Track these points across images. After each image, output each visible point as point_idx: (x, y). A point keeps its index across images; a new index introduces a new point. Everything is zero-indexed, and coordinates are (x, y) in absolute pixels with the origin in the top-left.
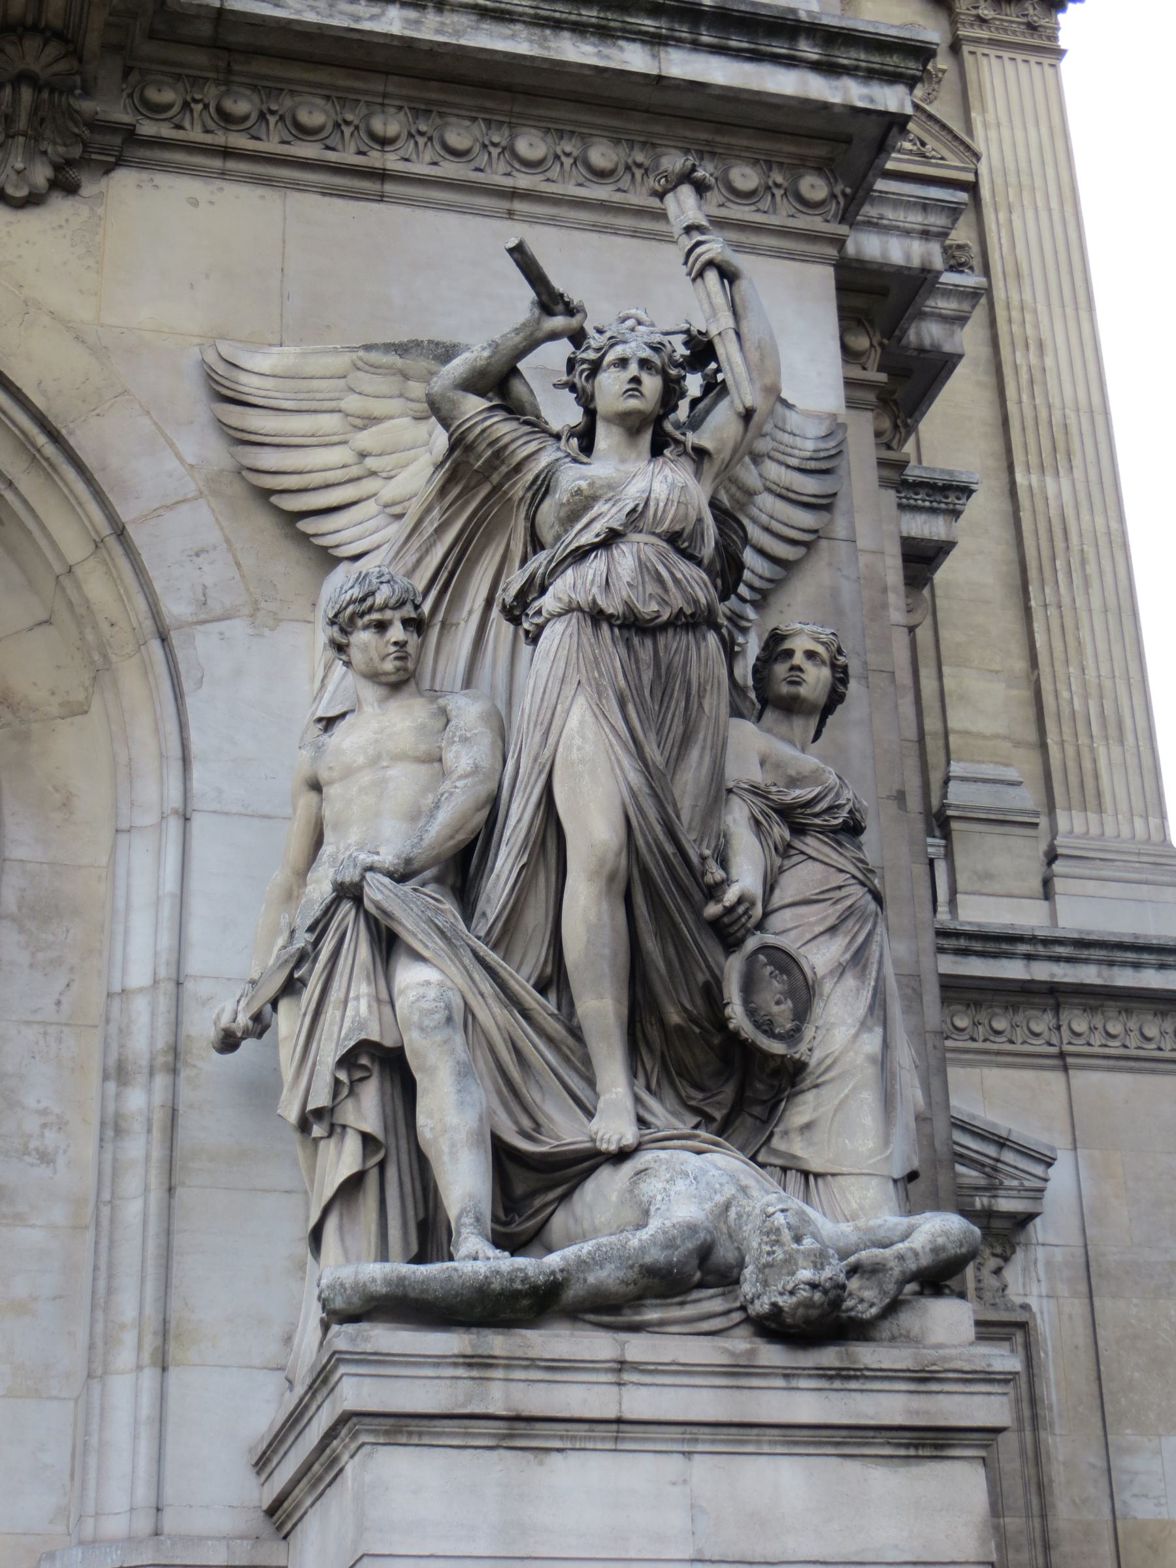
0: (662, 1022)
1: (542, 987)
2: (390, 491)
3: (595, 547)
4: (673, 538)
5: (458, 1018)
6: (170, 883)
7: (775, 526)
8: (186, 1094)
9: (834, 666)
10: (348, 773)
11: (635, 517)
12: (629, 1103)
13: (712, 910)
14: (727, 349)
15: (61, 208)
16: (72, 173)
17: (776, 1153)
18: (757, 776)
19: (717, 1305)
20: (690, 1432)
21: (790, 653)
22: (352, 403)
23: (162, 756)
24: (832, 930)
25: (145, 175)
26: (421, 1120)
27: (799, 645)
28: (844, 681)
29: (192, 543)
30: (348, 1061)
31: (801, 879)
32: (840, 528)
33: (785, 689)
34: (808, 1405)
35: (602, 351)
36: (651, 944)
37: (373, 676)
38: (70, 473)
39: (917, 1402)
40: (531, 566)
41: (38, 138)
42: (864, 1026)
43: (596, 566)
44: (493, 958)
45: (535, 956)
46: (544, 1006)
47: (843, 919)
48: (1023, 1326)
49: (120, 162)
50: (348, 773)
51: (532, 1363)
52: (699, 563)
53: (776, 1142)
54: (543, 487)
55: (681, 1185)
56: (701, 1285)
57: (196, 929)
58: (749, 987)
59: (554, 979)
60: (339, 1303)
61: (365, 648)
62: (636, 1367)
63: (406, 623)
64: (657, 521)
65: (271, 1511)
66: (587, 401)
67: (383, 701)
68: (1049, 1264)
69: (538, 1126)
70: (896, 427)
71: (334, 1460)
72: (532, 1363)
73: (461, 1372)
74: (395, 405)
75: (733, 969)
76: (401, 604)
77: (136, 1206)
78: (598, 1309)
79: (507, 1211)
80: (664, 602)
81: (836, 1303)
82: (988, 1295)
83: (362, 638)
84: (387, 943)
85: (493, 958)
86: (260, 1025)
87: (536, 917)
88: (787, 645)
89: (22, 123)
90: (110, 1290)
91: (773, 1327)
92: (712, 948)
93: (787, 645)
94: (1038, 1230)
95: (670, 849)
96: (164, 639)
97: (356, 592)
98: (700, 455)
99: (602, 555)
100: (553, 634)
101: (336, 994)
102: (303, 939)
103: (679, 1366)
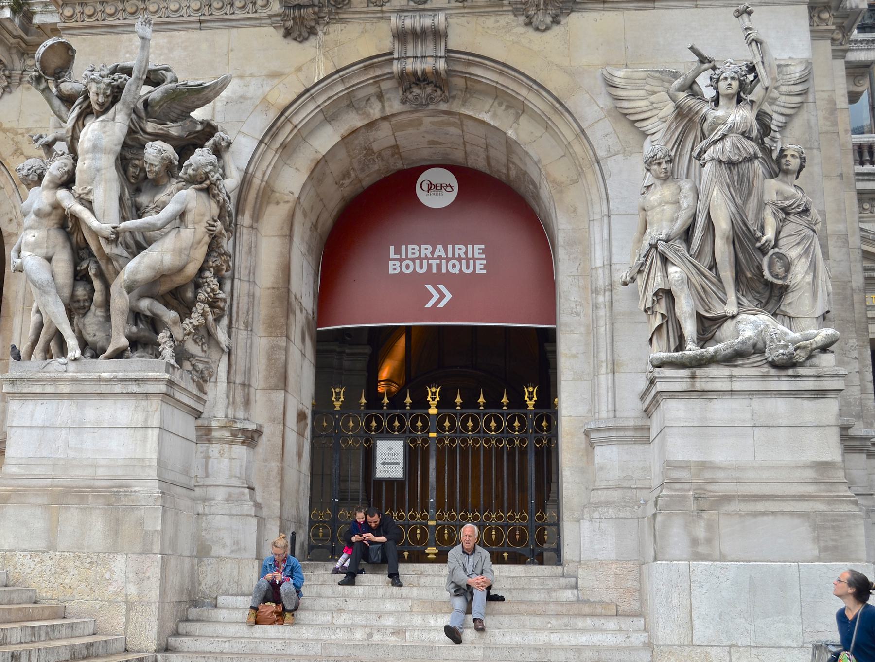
0: (746, 277)
1: (710, 269)
2: (662, 114)
3: (719, 140)
4: (743, 134)
5: (686, 281)
6: (606, 237)
7: (786, 105)
8: (615, 297)
9: (801, 158)
10: (653, 208)
11: (731, 130)
12: (735, 301)
13: (758, 245)
14: (760, 69)
15: (556, 29)
16: (558, 18)
17: (782, 311)
18: (775, 198)
19: (759, 359)
20: (751, 394)
21: (786, 156)
22: (648, 87)
23: (601, 198)
24: (798, 244)
25: (580, 14)
26: (676, 310)
27: (789, 153)
28: (805, 162)
29: (604, 135)
30: (656, 294)
31: (788, 228)
32: (811, 99)
33: (785, 167)
35: (720, 75)
36: (740, 255)
37: (658, 178)
38: (566, 114)
40: (702, 144)
41: (547, 10)
42: (806, 273)
43: (719, 145)
44: (695, 262)
45: (708, 260)
46: (711, 274)
47: (802, 240)
49: (572, 11)
50: (653, 208)
51: (707, 377)
52: (752, 139)
53: (781, 308)
54: (704, 119)
55: (748, 326)
56: (754, 353)
57: (614, 250)
58: (771, 265)
59: (713, 266)
60: (656, 363)
61: (655, 170)
62: (736, 377)
63: (666, 162)
64: (738, 129)
65: (645, 411)
66: (716, 89)
67: (662, 185)
69: (710, 309)
70: (844, 36)
71: (657, 401)
72: (707, 377)
74: (661, 89)
75: (765, 261)
76: (665, 157)
77: (603, 329)
78: (724, 361)
79: (703, 331)
80: (740, 155)
81: (791, 358)
83: (655, 167)
84: (665, 260)
85: (695, 262)
86: (633, 279)
87: (708, 249)
88: (785, 153)
89: (542, 6)
90: (598, 352)
91: (773, 365)
92: (757, 256)
93: (785, 153)
95: (744, 228)
96: (598, 163)
97: (652, 155)
98: (752, 102)
99: (721, 142)
100: (708, 165)
101: (652, 275)
102: (642, 260)
103: (747, 376)
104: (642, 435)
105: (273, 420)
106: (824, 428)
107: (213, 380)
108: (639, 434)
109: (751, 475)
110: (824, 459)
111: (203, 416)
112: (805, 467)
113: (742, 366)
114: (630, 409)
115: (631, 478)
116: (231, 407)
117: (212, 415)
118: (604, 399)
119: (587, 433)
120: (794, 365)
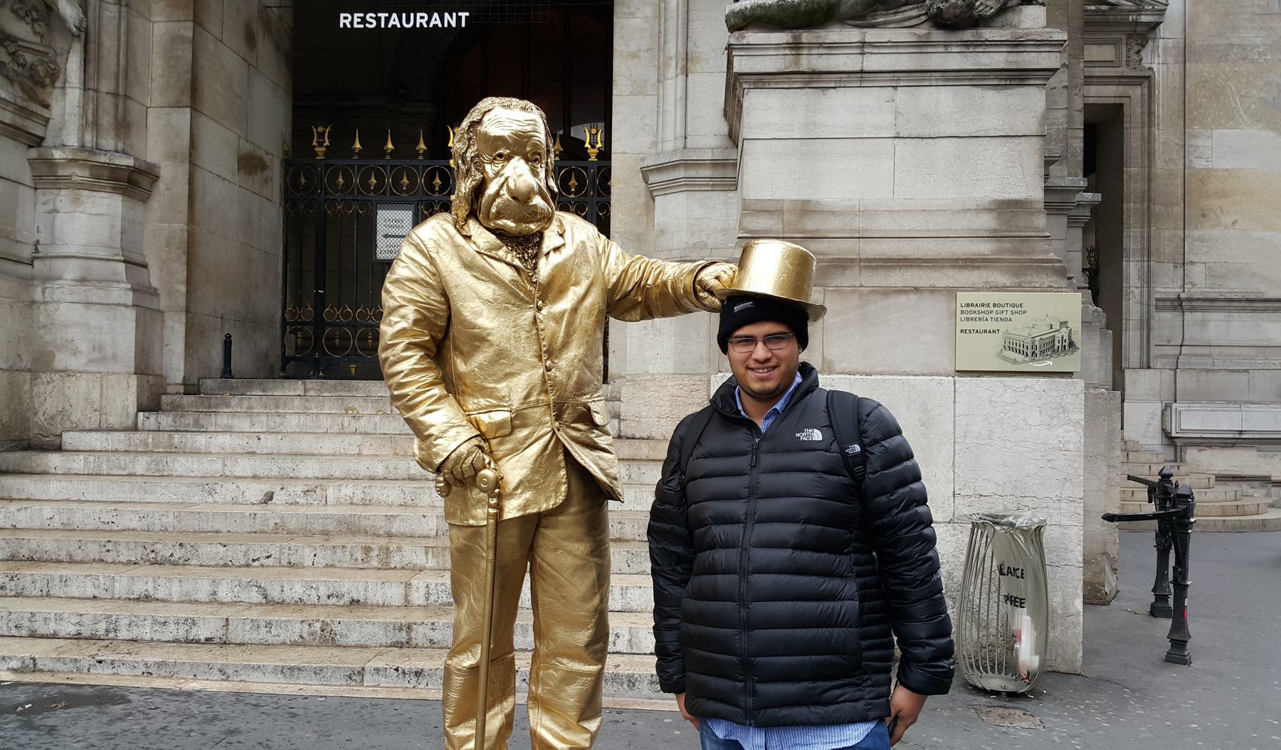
19: (914, 13)
34: (956, 60)
39: (1013, 57)
48: (1148, 78)
62: (872, 45)
68: (1165, 48)
73: (787, 52)
78: (853, 18)
82: (1132, 64)
94: (1162, 31)
104: (725, 172)
105: (172, 156)
106: (1017, 140)
107: (58, 84)
108: (719, 173)
109: (884, 224)
110: (1014, 196)
111: (45, 144)
112: (979, 210)
113: (883, 25)
114: (708, 132)
115: (705, 246)
116: (89, 129)
117: (58, 142)
118: (670, 119)
119: (646, 173)
120: (978, 22)
